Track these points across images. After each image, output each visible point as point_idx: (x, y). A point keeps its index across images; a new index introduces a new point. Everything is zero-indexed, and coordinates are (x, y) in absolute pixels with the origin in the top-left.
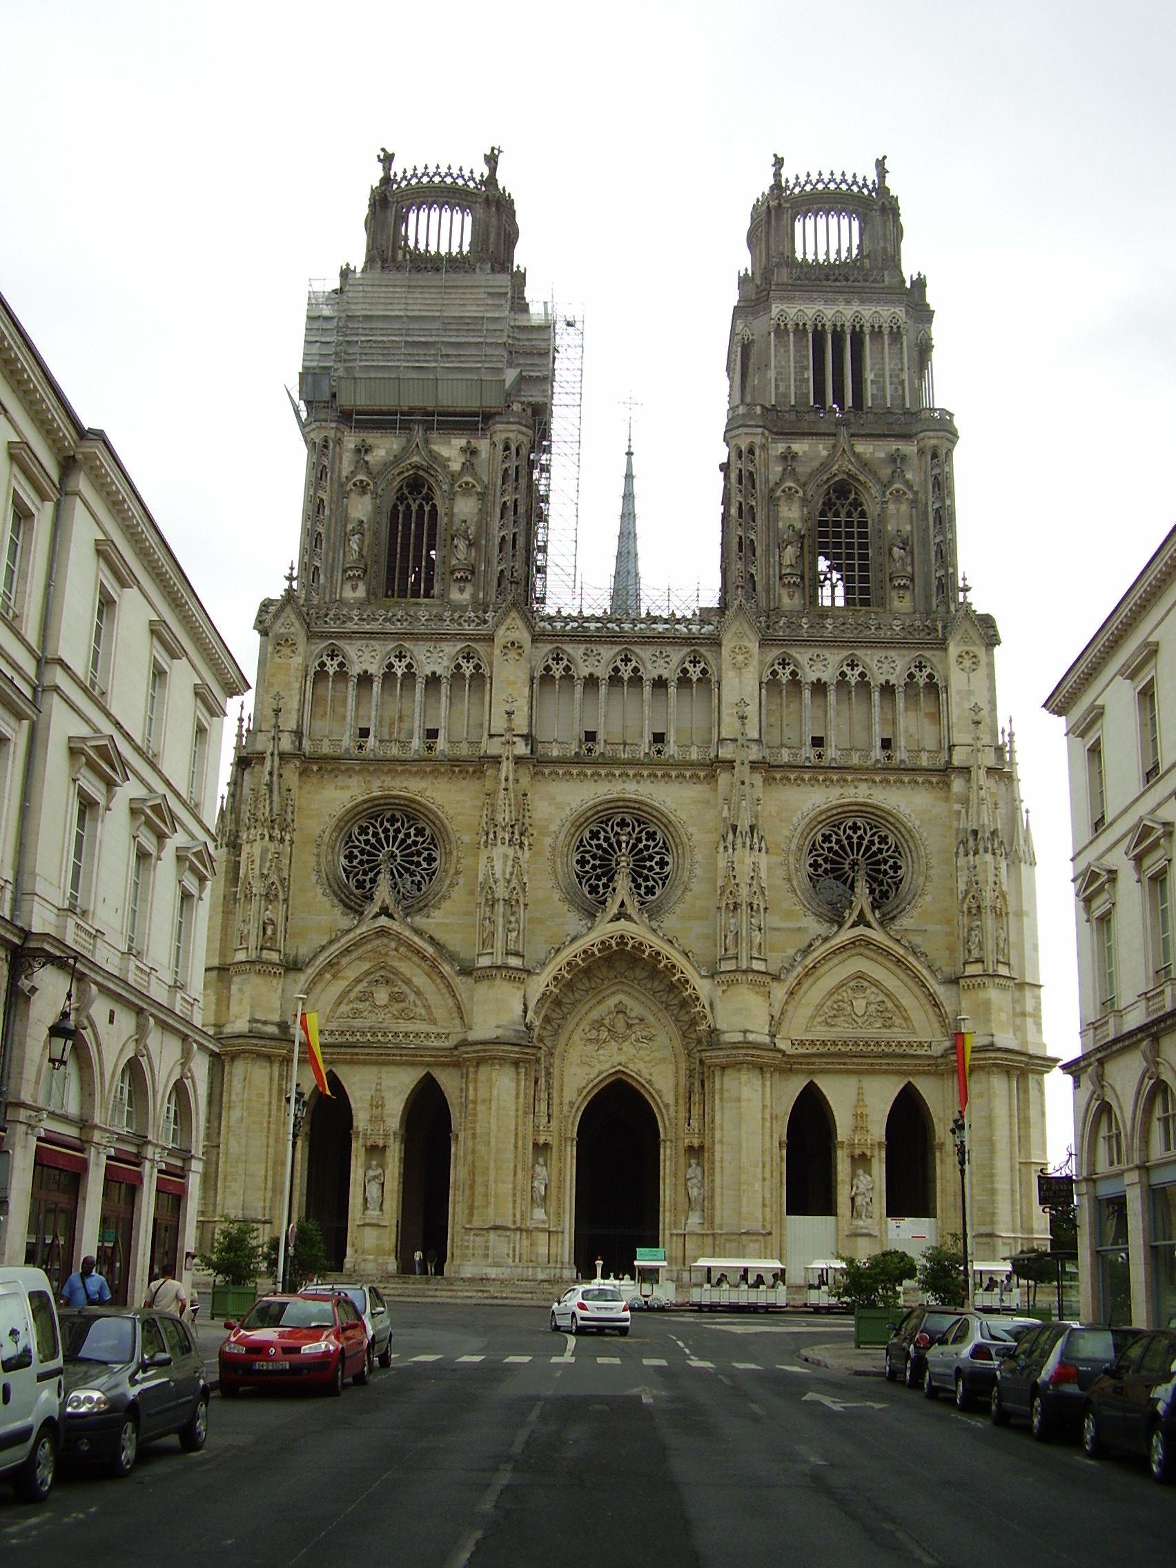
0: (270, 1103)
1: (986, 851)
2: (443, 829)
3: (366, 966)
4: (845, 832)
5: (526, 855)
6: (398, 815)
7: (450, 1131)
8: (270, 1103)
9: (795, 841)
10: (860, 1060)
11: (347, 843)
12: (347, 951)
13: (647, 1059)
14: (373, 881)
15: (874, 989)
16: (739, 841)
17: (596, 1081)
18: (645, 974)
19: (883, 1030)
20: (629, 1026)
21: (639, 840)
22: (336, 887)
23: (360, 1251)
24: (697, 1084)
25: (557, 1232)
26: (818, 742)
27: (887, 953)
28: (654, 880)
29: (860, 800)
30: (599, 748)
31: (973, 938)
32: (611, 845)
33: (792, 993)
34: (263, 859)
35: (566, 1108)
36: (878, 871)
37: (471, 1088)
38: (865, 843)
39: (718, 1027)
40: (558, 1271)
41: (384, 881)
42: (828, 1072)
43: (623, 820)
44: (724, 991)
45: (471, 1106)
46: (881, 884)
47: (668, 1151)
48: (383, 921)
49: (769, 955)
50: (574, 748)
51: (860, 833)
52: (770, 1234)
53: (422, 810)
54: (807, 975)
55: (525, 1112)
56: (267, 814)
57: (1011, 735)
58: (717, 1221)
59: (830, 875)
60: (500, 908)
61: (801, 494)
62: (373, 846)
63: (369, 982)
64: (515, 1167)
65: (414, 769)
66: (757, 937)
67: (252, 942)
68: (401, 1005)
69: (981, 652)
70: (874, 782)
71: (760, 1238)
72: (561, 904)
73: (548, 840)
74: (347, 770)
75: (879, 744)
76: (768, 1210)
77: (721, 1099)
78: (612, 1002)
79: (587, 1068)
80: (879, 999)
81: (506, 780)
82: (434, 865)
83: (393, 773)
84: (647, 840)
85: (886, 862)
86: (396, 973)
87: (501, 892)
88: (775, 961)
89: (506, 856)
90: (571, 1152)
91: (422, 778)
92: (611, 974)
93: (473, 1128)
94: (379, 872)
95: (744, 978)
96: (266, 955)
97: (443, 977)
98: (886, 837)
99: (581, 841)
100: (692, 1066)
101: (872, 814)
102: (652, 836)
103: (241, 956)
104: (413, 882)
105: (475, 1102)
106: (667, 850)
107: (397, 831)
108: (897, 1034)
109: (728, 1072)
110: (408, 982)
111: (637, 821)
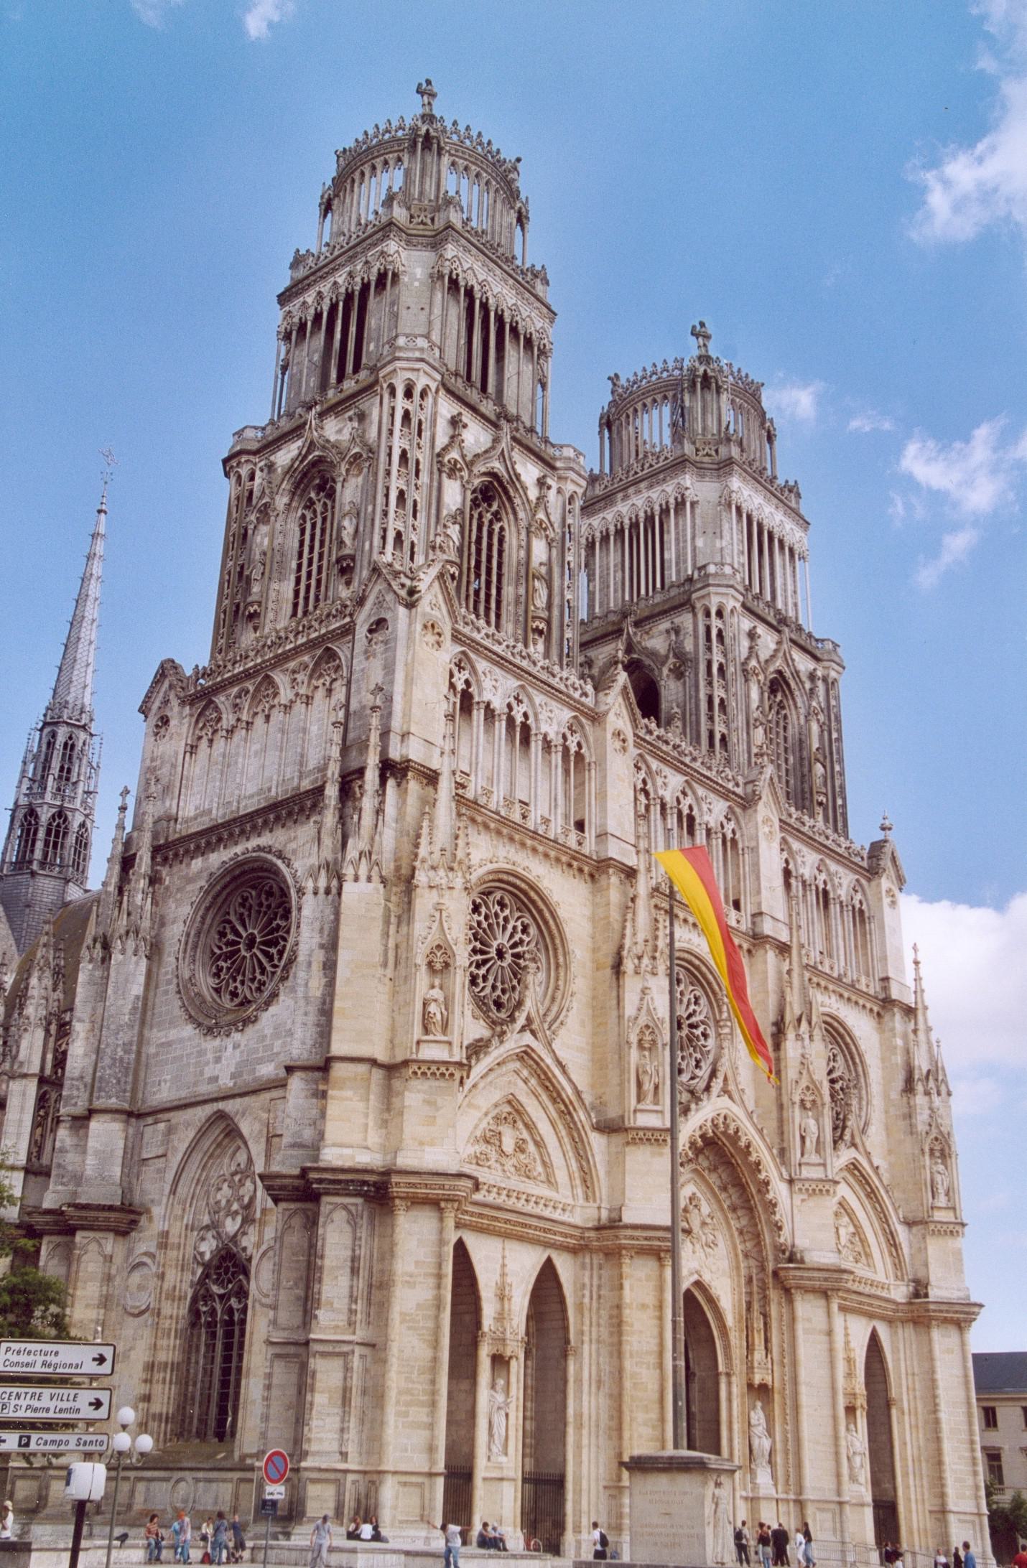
3: (497, 1096)
20: (704, 1224)
44: (803, 1200)
53: (540, 903)
61: (761, 677)
63: (497, 1118)
68: (522, 1157)
69: (896, 891)
70: (841, 996)
107: (506, 919)
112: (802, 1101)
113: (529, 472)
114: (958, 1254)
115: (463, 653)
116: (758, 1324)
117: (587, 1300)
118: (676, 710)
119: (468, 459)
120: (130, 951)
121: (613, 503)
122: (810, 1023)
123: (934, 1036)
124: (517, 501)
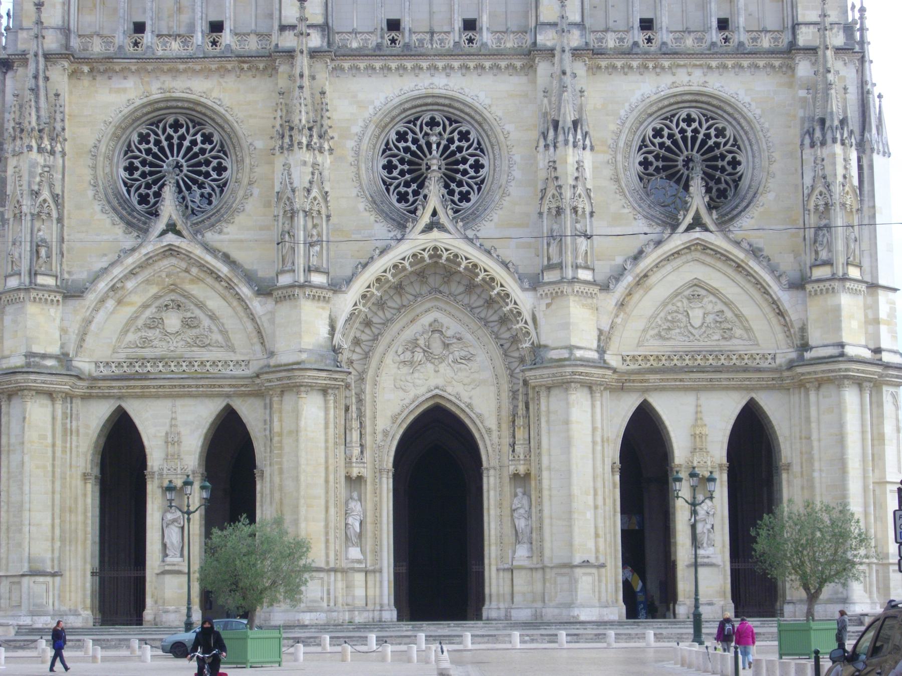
0: (54, 445)
1: (834, 141)
2: (232, 134)
3: (154, 290)
4: (677, 125)
5: (326, 160)
6: (182, 120)
7: (254, 466)
8: (54, 445)
9: (623, 137)
10: (697, 373)
11: (126, 153)
12: (133, 273)
13: (466, 381)
14: (158, 195)
15: (711, 298)
16: (561, 138)
17: (412, 407)
18: (461, 289)
19: (723, 343)
20: (446, 346)
21: (451, 141)
22: (115, 203)
23: (160, 602)
24: (521, 406)
25: (374, 571)
26: (647, 25)
27: (725, 258)
28: (469, 185)
29: (695, 88)
30: (405, 38)
31: (820, 239)
32: (420, 148)
33: (622, 305)
34: (32, 174)
35: (379, 437)
36: (715, 168)
37: (276, 419)
38: (701, 136)
39: (542, 343)
40: (377, 614)
41: (169, 193)
42: (663, 389)
43: (433, 119)
45: (276, 439)
46: (718, 181)
47: (492, 480)
48: (171, 238)
49: (598, 265)
50: (373, 41)
51: (695, 125)
52: (603, 566)
53: (209, 113)
54: (638, 284)
55: (336, 443)
56: (34, 124)
57: (862, 10)
58: (547, 553)
59: (663, 174)
60: (300, 219)
62: (155, 156)
63: (158, 307)
64: (327, 502)
65: (198, 67)
66: (583, 243)
67: (24, 267)
68: (194, 332)
70: (710, 67)
71: (594, 571)
72: (367, 214)
73: (351, 144)
74: (122, 70)
75: (715, 24)
76: (601, 541)
77: (548, 422)
78: (427, 320)
79: (401, 394)
80: (717, 308)
81: (301, 76)
82: (225, 175)
83: (174, 72)
84: (460, 140)
85: (723, 157)
86: (187, 296)
87: (300, 202)
88: (604, 269)
89: (305, 163)
90: (387, 485)
91: (207, 77)
92: (425, 289)
93: (280, 463)
94: (163, 185)
95: (570, 290)
96: (41, 280)
97: (240, 299)
98: (724, 129)
99: (387, 144)
100: (516, 388)
101: (708, 104)
102: (464, 136)
103: (13, 282)
104: (202, 195)
105: (280, 435)
106: (482, 151)
107: (182, 138)
108: (738, 344)
109: (554, 392)
110: (201, 306)
111: (449, 119)
112: (549, 209)
117: (268, 433)
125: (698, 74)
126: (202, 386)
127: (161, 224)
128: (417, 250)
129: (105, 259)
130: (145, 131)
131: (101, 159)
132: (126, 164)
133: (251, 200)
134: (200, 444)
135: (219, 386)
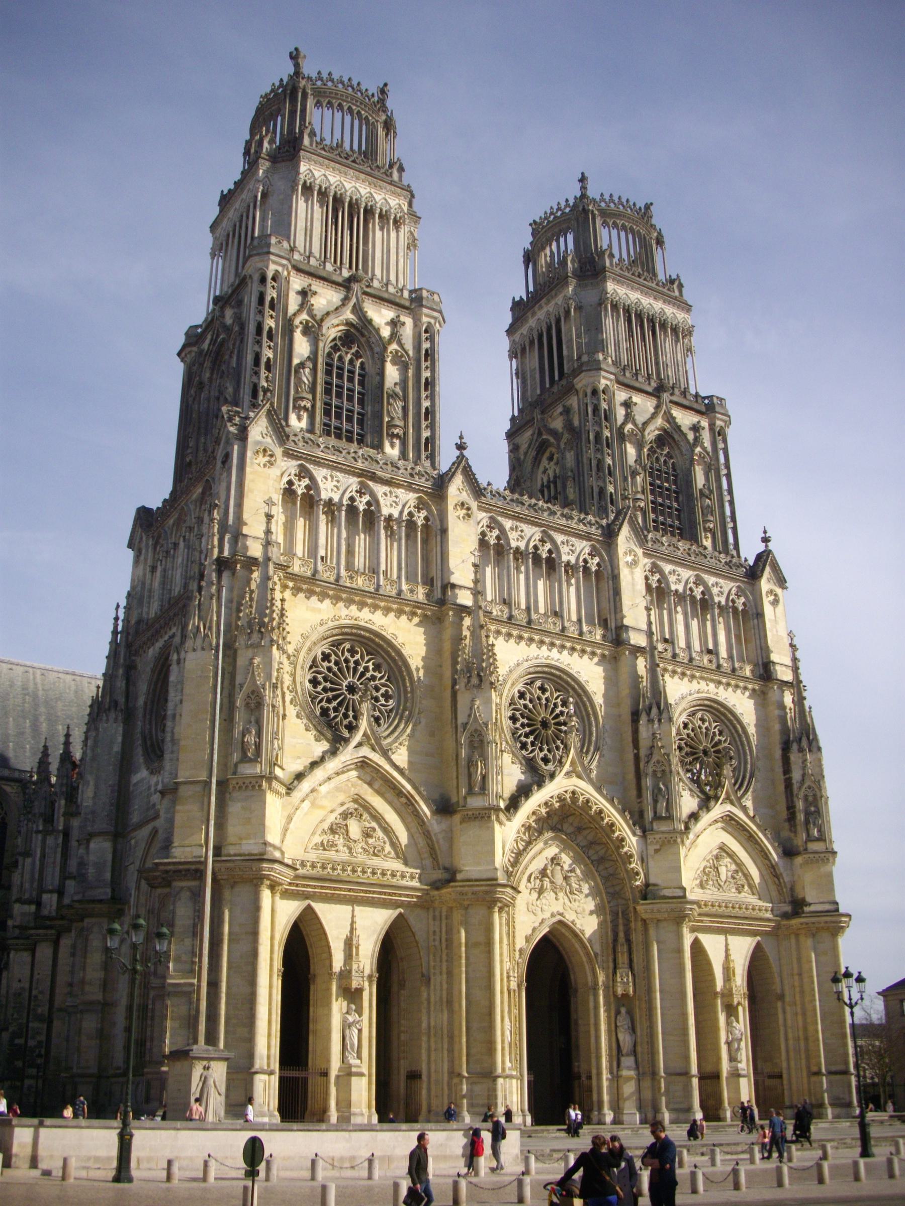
3: (341, 797)
24: (621, 935)
35: (517, 954)
44: (656, 851)
48: (366, 751)
68: (371, 841)
107: (357, 663)
112: (654, 771)
113: (380, 317)
114: (830, 876)
115: (301, 466)
116: (622, 949)
117: (437, 943)
118: (570, 474)
119: (318, 317)
120: (111, 720)
121: (526, 321)
122: (659, 708)
123: (807, 703)
124: (373, 340)
125: (712, 686)
126: (385, 893)
127: (358, 737)
128: (561, 791)
129: (299, 761)
130: (327, 651)
131: (299, 667)
132: (309, 676)
133: (419, 727)
134: (377, 949)
135: (400, 895)
